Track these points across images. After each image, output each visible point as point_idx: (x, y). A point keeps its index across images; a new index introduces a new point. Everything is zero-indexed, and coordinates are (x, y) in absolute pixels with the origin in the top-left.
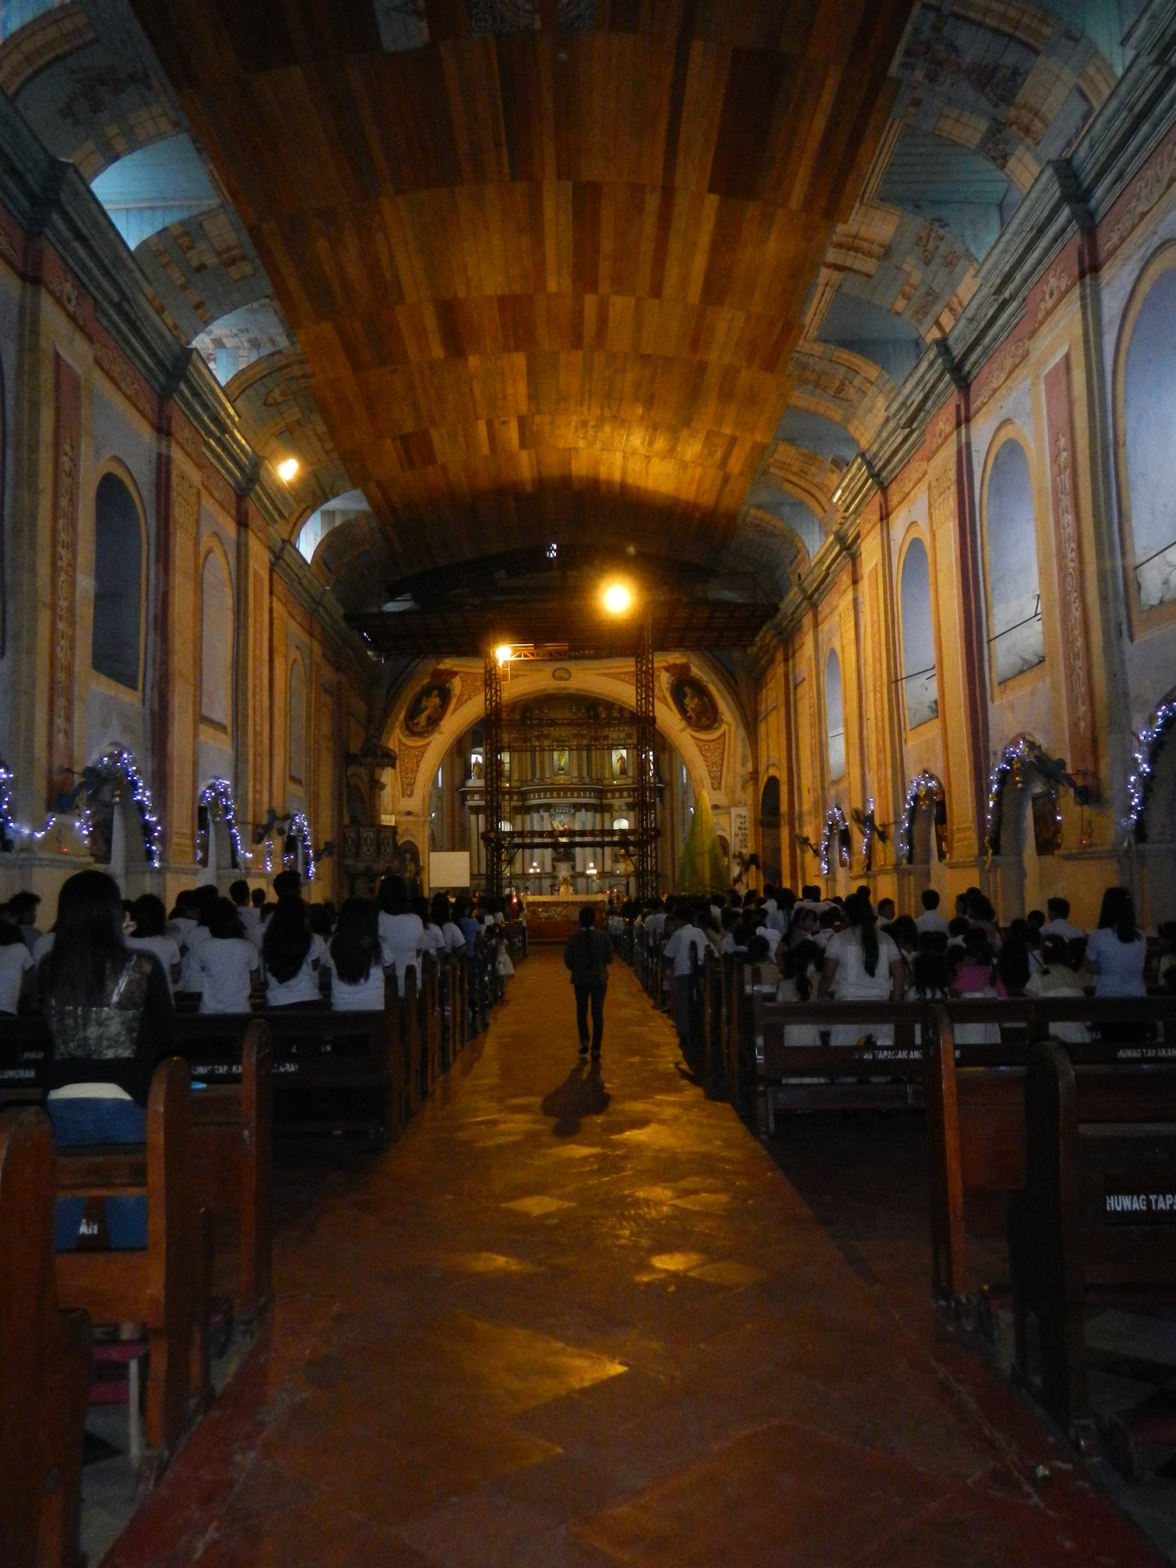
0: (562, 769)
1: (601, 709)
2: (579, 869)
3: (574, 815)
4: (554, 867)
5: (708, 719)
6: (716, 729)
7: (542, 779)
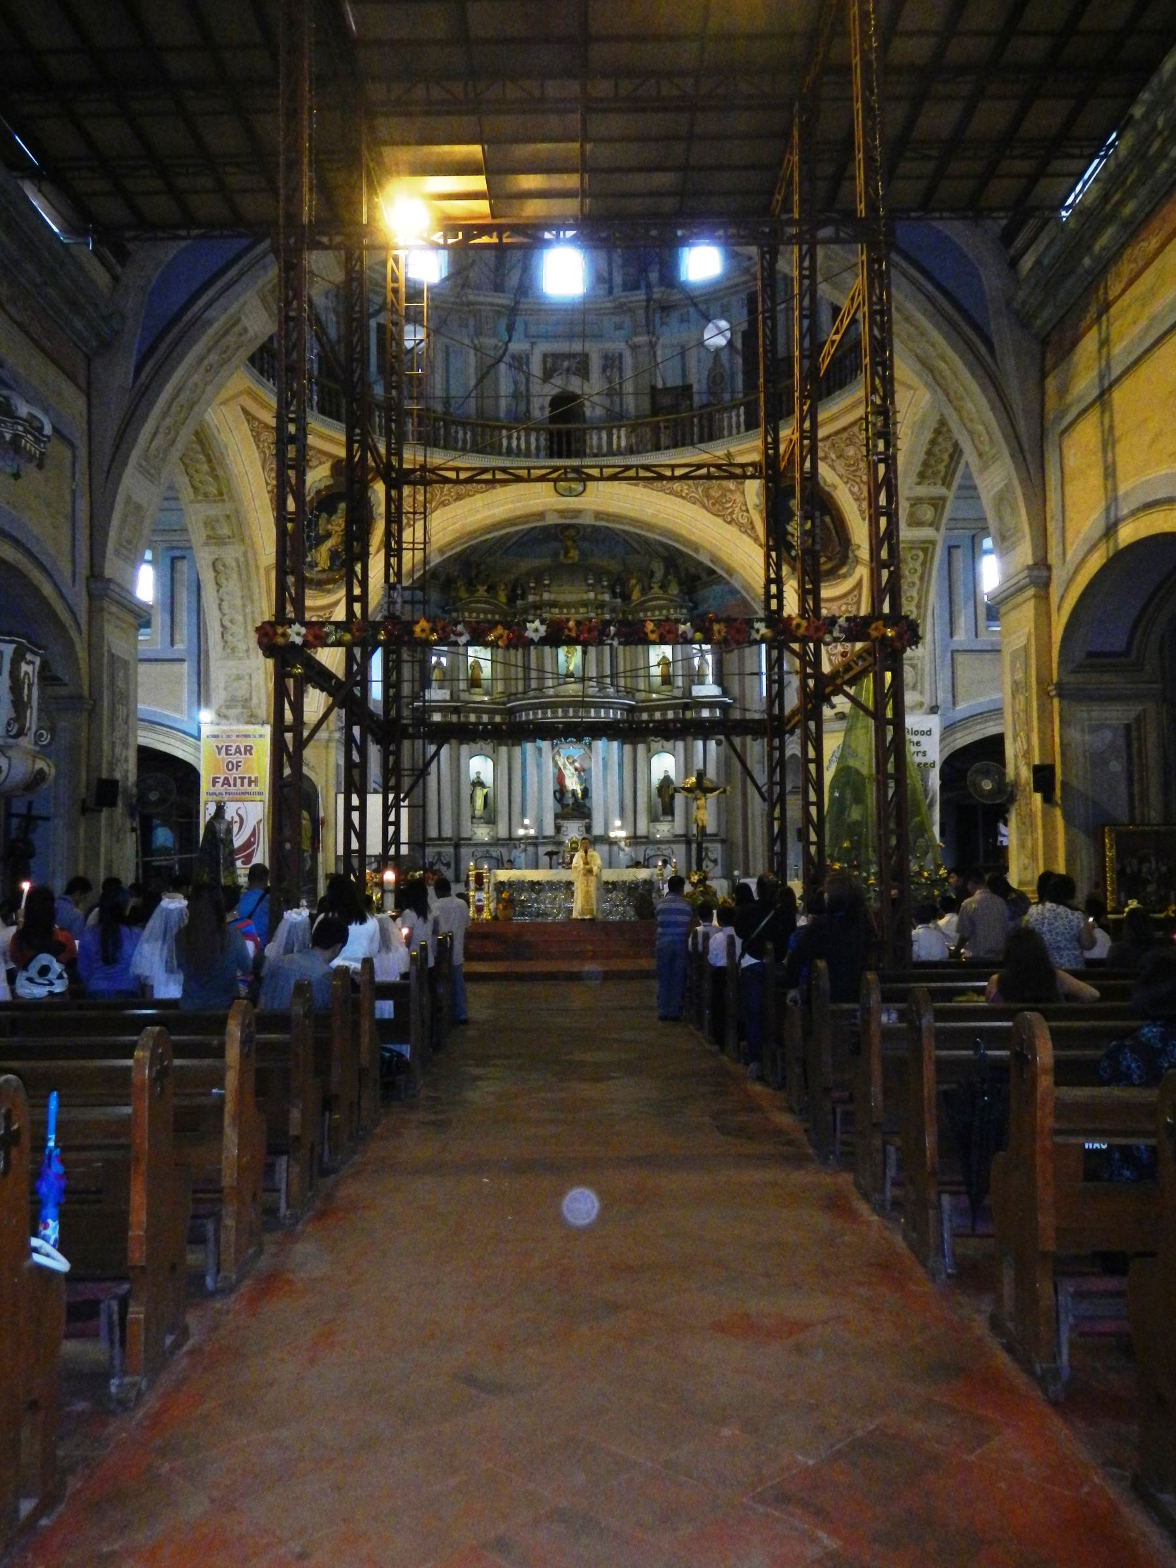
0: (572, 675)
1: (633, 581)
2: (598, 830)
3: (590, 746)
4: (558, 829)
5: (830, 559)
6: (845, 576)
7: (540, 689)
